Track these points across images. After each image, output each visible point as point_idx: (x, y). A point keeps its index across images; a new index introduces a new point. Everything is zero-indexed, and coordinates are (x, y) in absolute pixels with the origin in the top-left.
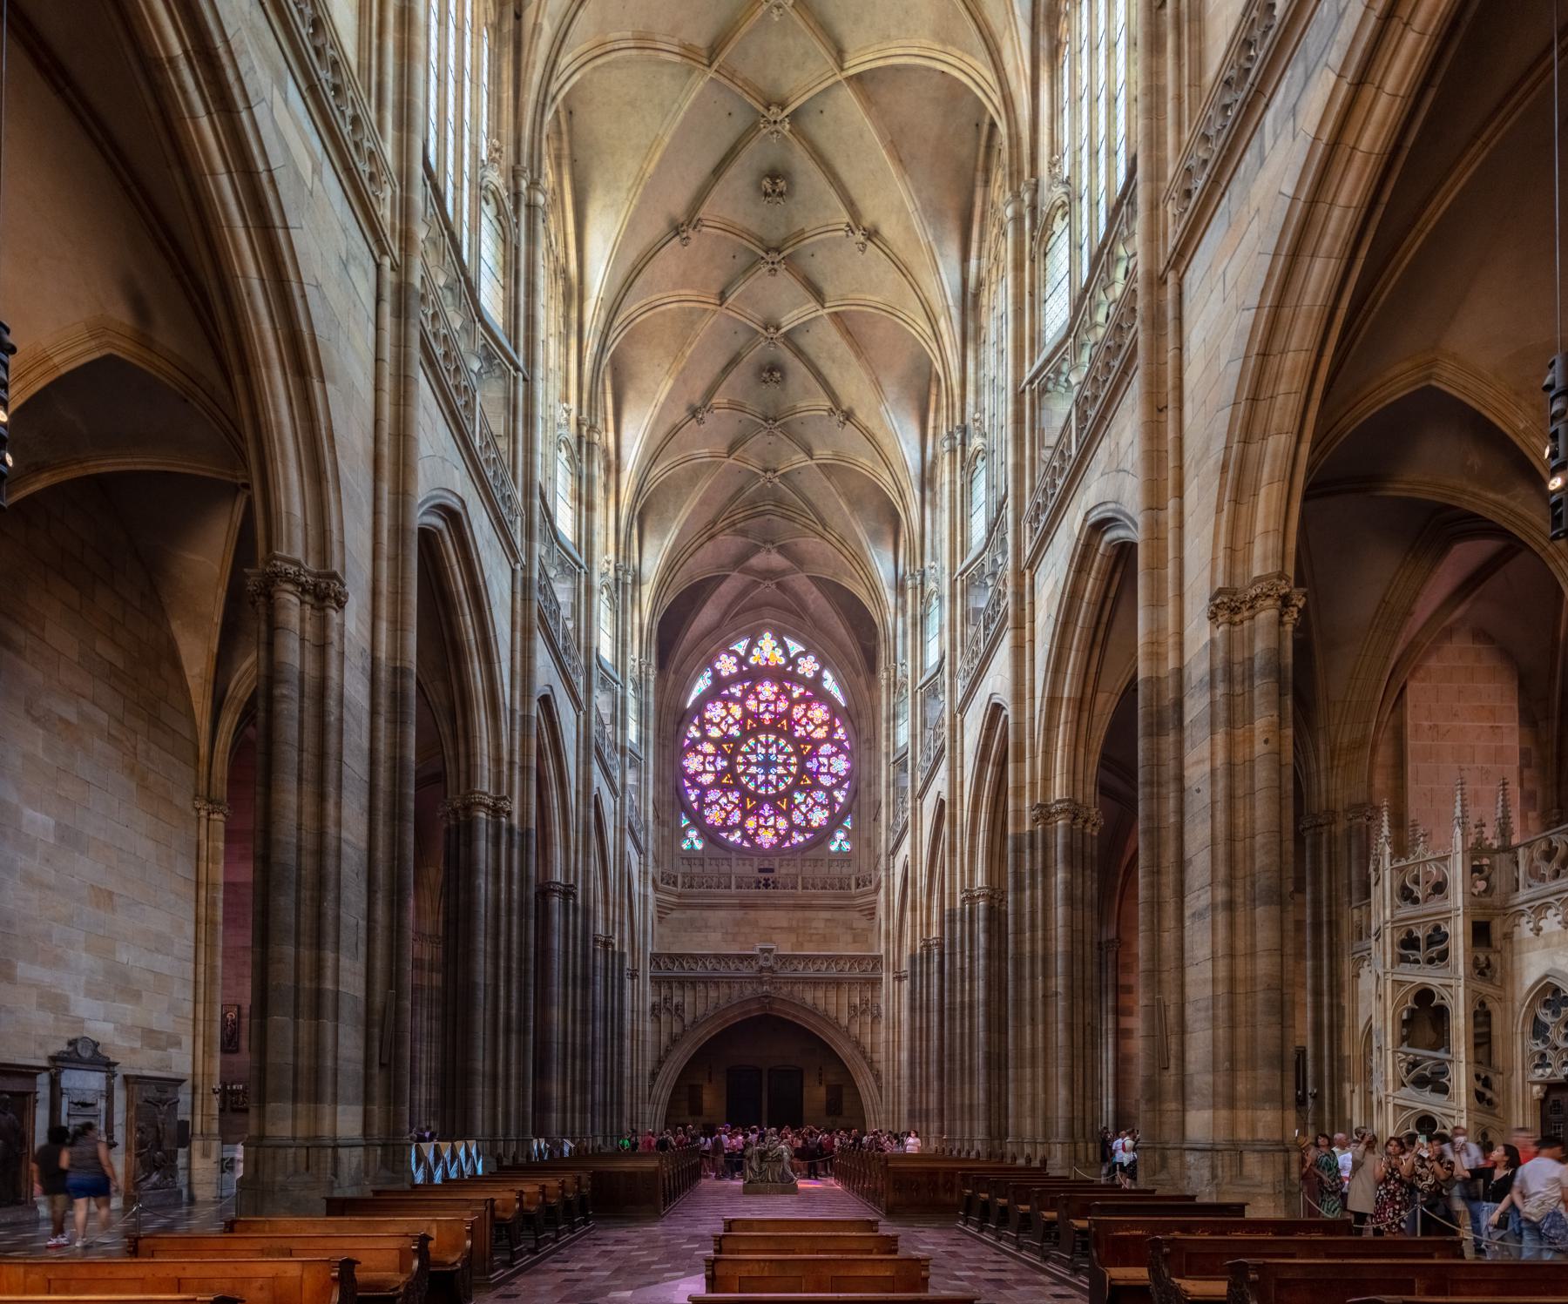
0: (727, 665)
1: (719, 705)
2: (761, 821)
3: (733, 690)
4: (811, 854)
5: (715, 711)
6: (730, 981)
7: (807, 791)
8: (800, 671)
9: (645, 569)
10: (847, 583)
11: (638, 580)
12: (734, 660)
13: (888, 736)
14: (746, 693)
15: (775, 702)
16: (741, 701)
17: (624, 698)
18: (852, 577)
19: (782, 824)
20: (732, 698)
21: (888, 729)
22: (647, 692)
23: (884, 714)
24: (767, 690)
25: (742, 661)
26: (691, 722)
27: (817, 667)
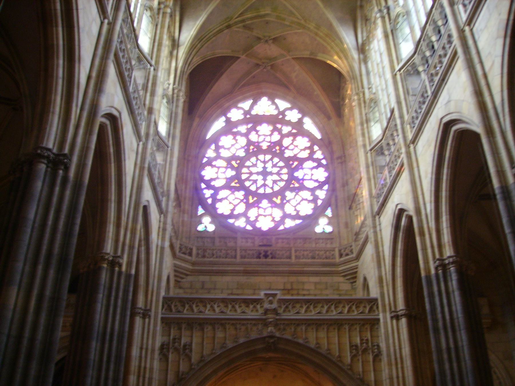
0: (235, 115)
5: (226, 141)
6: (235, 322)
8: (287, 118)
14: (249, 131)
16: (246, 135)
17: (155, 77)
22: (177, 106)
24: (265, 129)
25: (246, 113)
26: (209, 147)
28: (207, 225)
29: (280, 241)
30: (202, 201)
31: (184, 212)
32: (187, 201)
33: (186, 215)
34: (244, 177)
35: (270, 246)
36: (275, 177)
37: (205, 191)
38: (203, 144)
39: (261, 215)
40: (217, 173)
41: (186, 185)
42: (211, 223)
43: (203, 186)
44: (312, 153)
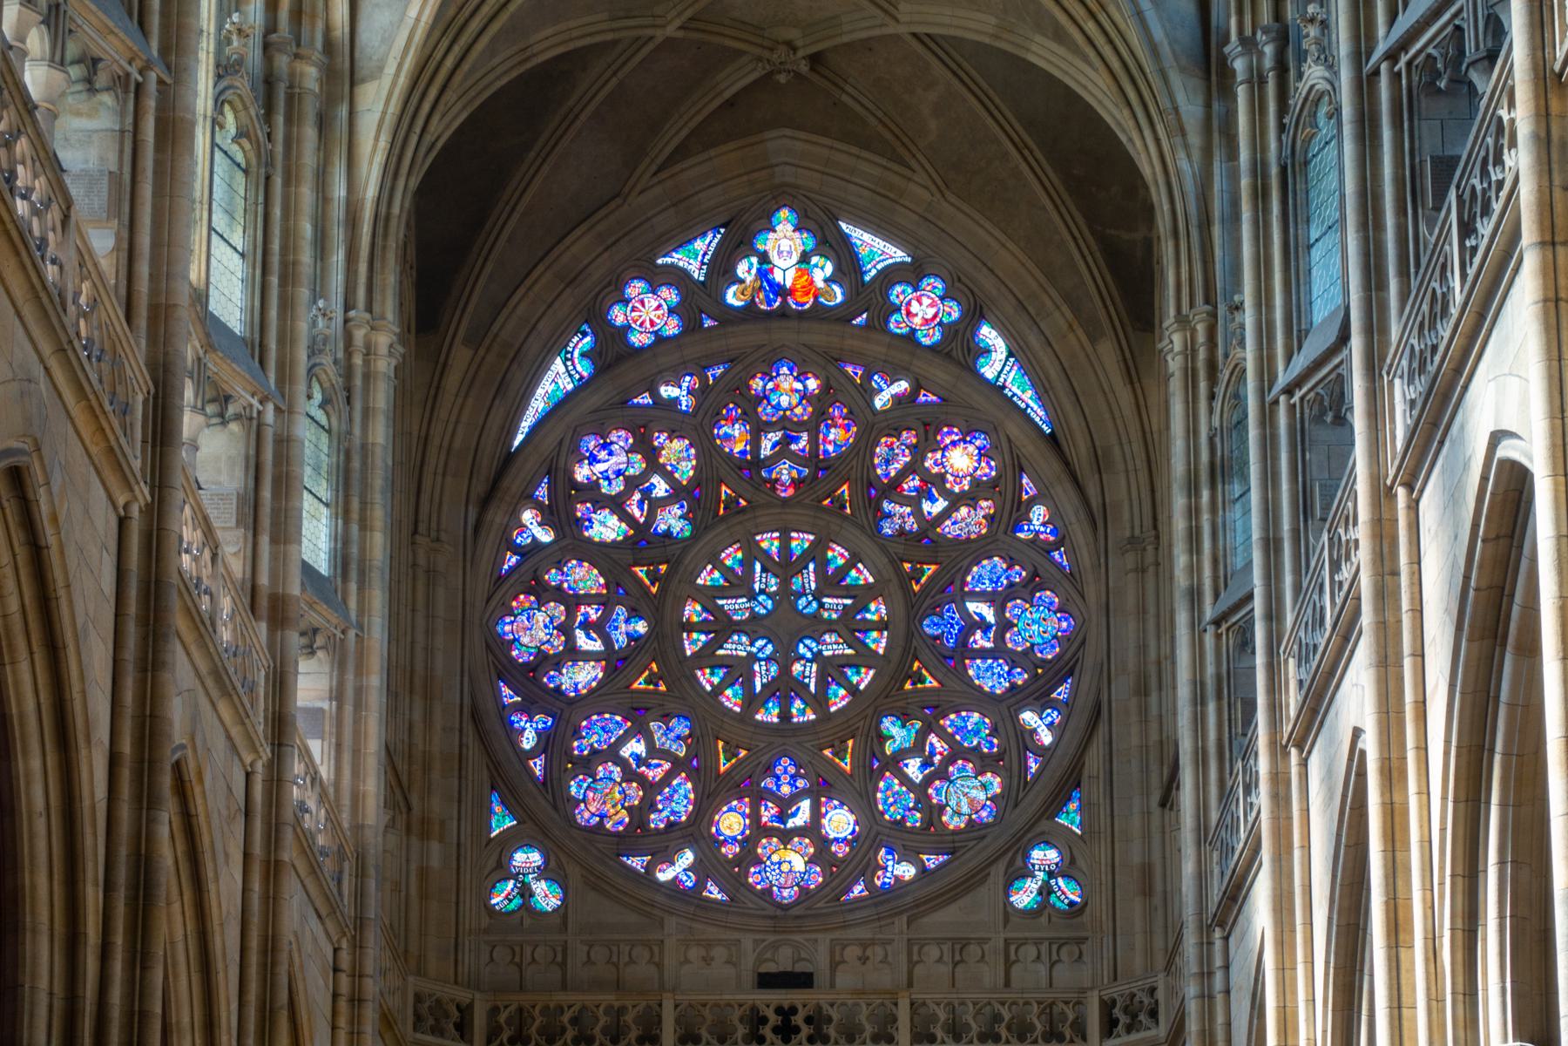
0: (647, 313)
1: (620, 439)
2: (768, 813)
3: (667, 391)
4: (948, 917)
5: (608, 462)
7: (930, 712)
8: (898, 324)
9: (369, 35)
10: (1044, 54)
11: (344, 71)
12: (670, 295)
13: (1194, 537)
15: (813, 428)
16: (697, 426)
18: (1060, 36)
19: (840, 822)
20: (669, 418)
21: (1193, 512)
23: (1178, 466)
24: (787, 390)
25: (697, 300)
27: (953, 312)
28: (531, 882)
29: (852, 952)
30: (503, 772)
31: (425, 836)
32: (436, 775)
33: (435, 846)
34: (693, 643)
35: (804, 980)
36: (833, 646)
37: (520, 721)
38: (497, 482)
39: (768, 832)
40: (565, 630)
41: (428, 697)
42: (543, 873)
43: (508, 695)
44: (1012, 513)
